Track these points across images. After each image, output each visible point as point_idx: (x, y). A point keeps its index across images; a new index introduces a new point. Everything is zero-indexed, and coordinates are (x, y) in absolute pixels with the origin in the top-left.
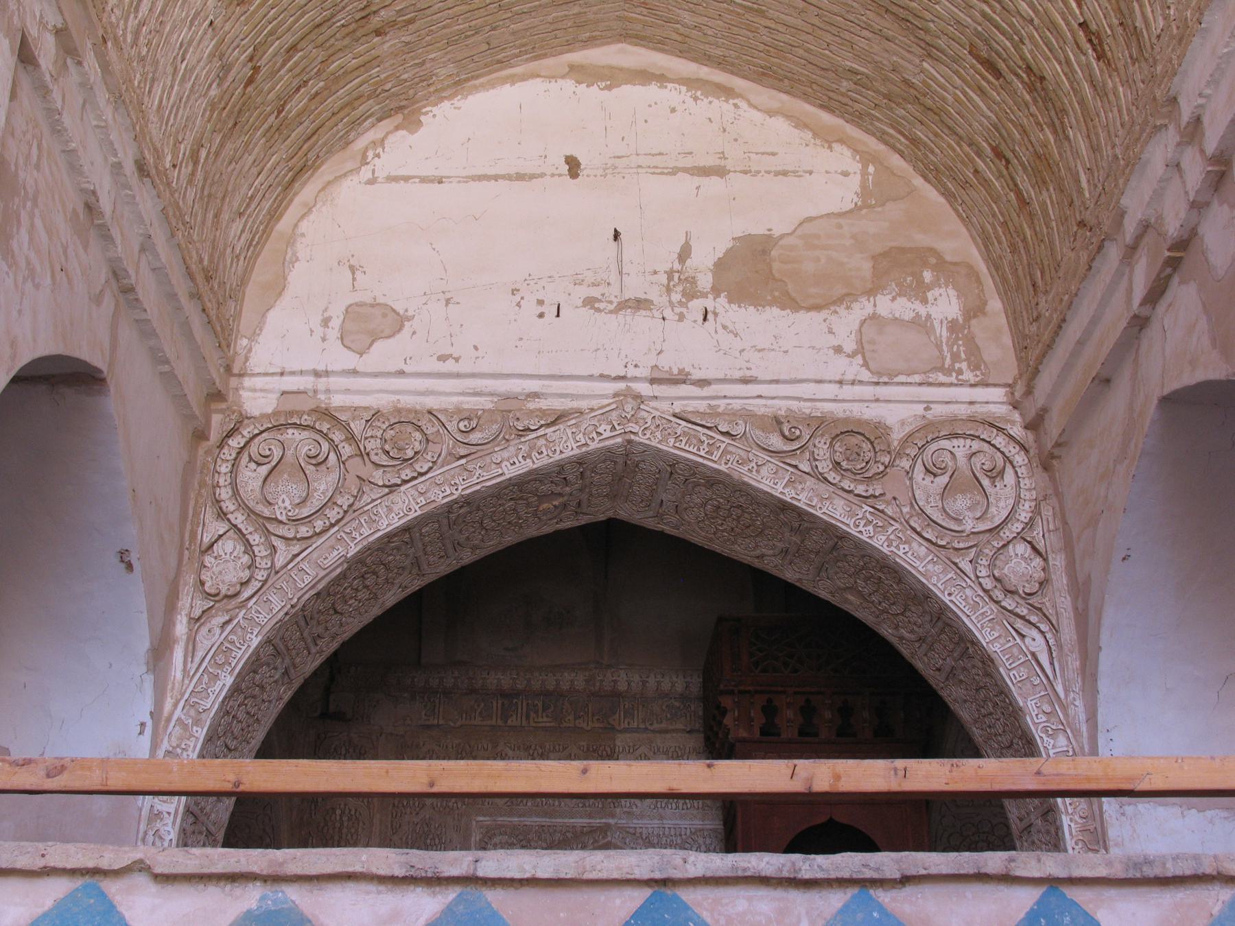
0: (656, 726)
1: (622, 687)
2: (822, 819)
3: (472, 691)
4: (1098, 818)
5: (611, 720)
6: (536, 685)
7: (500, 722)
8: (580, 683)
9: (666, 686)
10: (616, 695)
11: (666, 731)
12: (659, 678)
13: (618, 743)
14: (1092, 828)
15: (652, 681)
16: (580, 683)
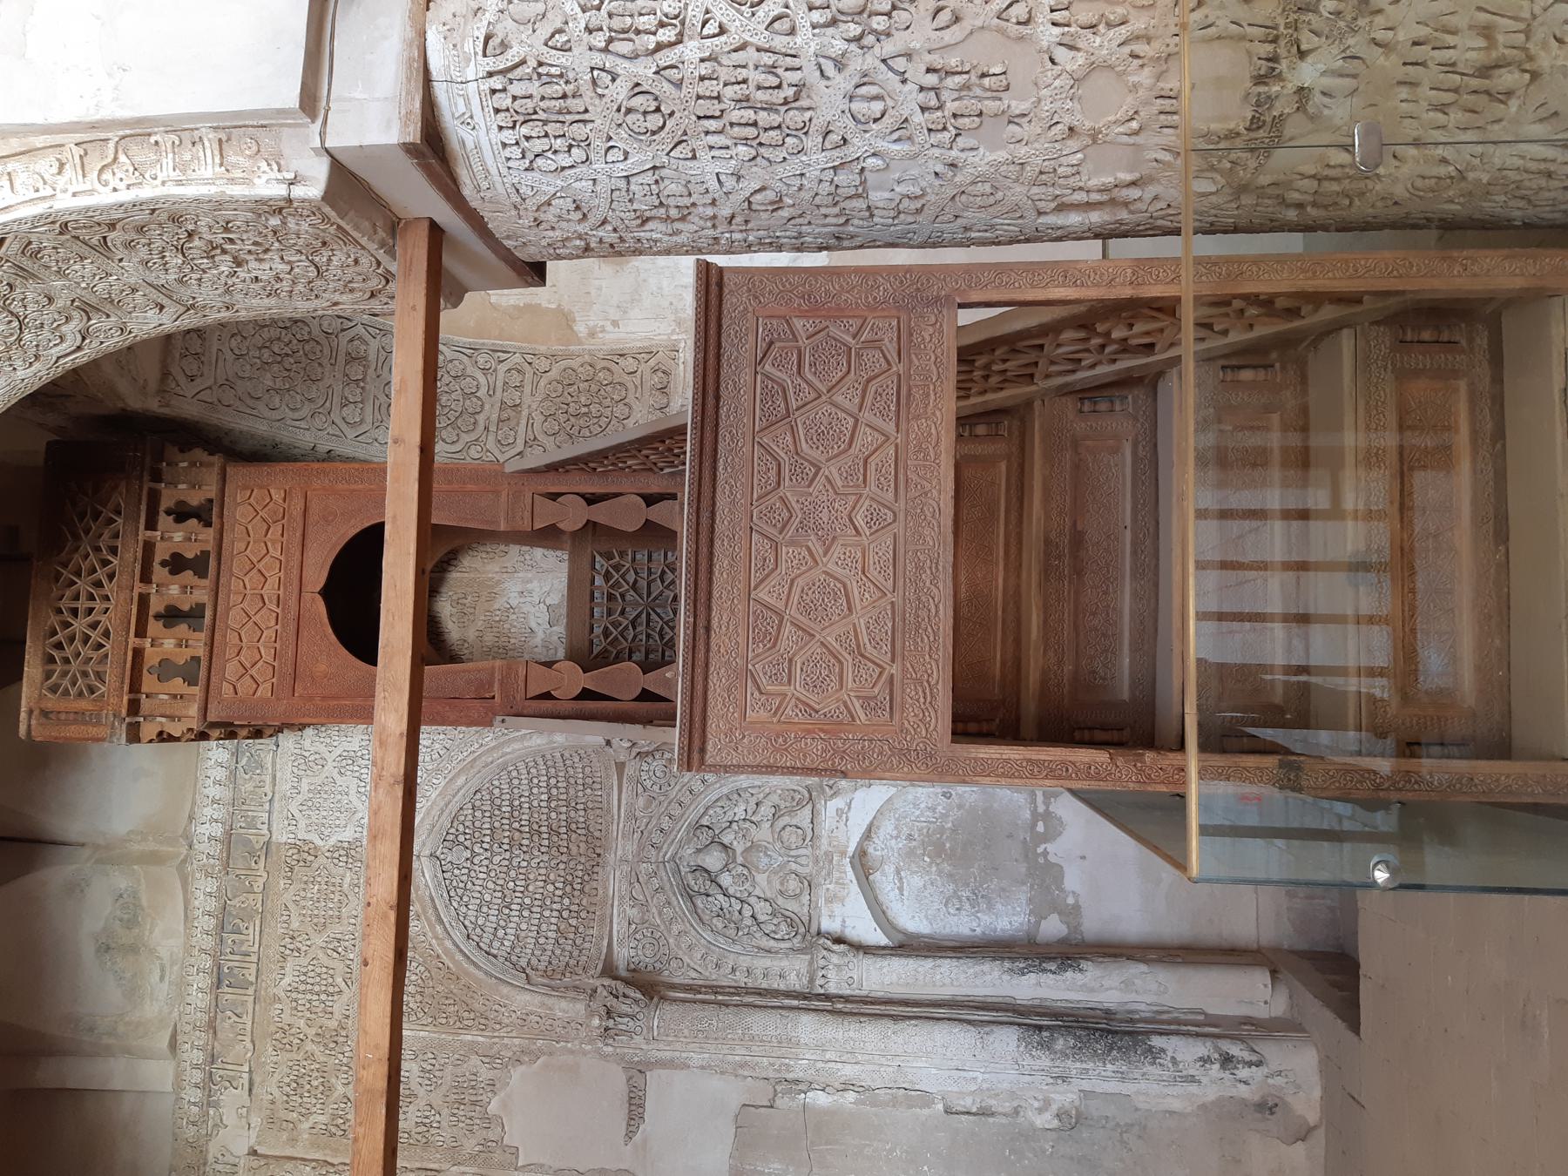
0: (268, 789)
1: (218, 830)
2: (321, 607)
3: (212, 1027)
4: (58, 139)
5: (258, 847)
6: (209, 942)
7: (251, 991)
8: (211, 886)
9: (220, 774)
10: (228, 839)
11: (274, 777)
12: (210, 782)
13: (284, 840)
14: (78, 151)
15: (214, 791)
16: (211, 886)
